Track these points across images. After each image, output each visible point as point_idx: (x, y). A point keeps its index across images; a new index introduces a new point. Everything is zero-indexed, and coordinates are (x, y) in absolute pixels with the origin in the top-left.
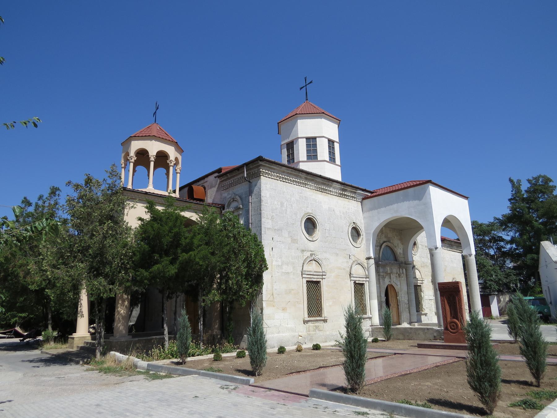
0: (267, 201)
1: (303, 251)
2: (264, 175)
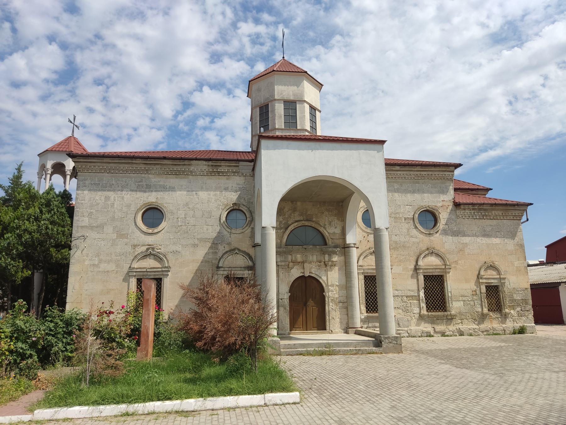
1: (135, 246)
2: (81, 171)
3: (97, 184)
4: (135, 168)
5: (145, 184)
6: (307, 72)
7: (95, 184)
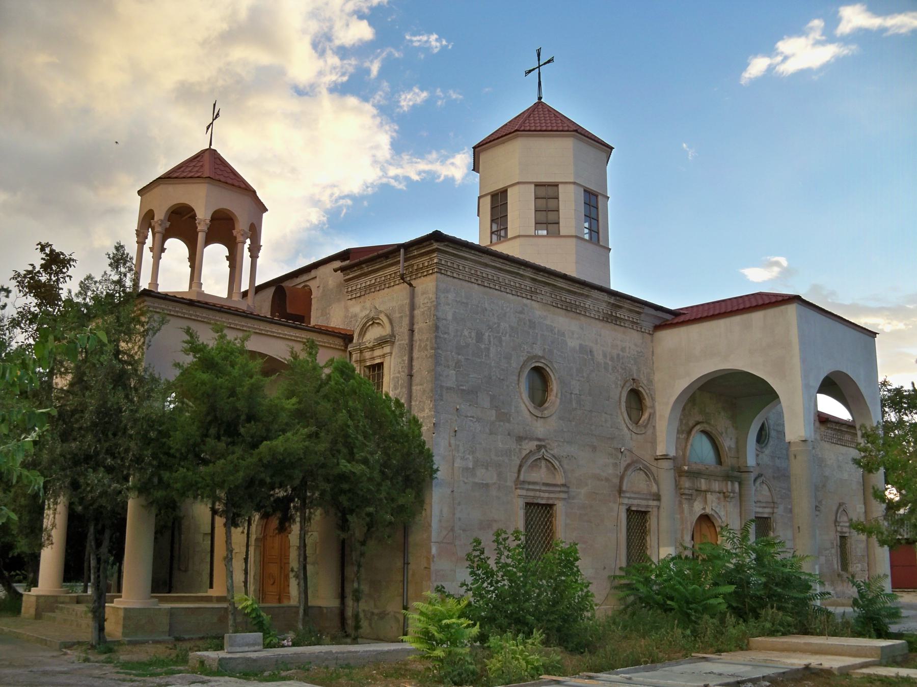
0: (448, 330)
1: (520, 439)
2: (443, 272)
3: (464, 303)
4: (517, 285)
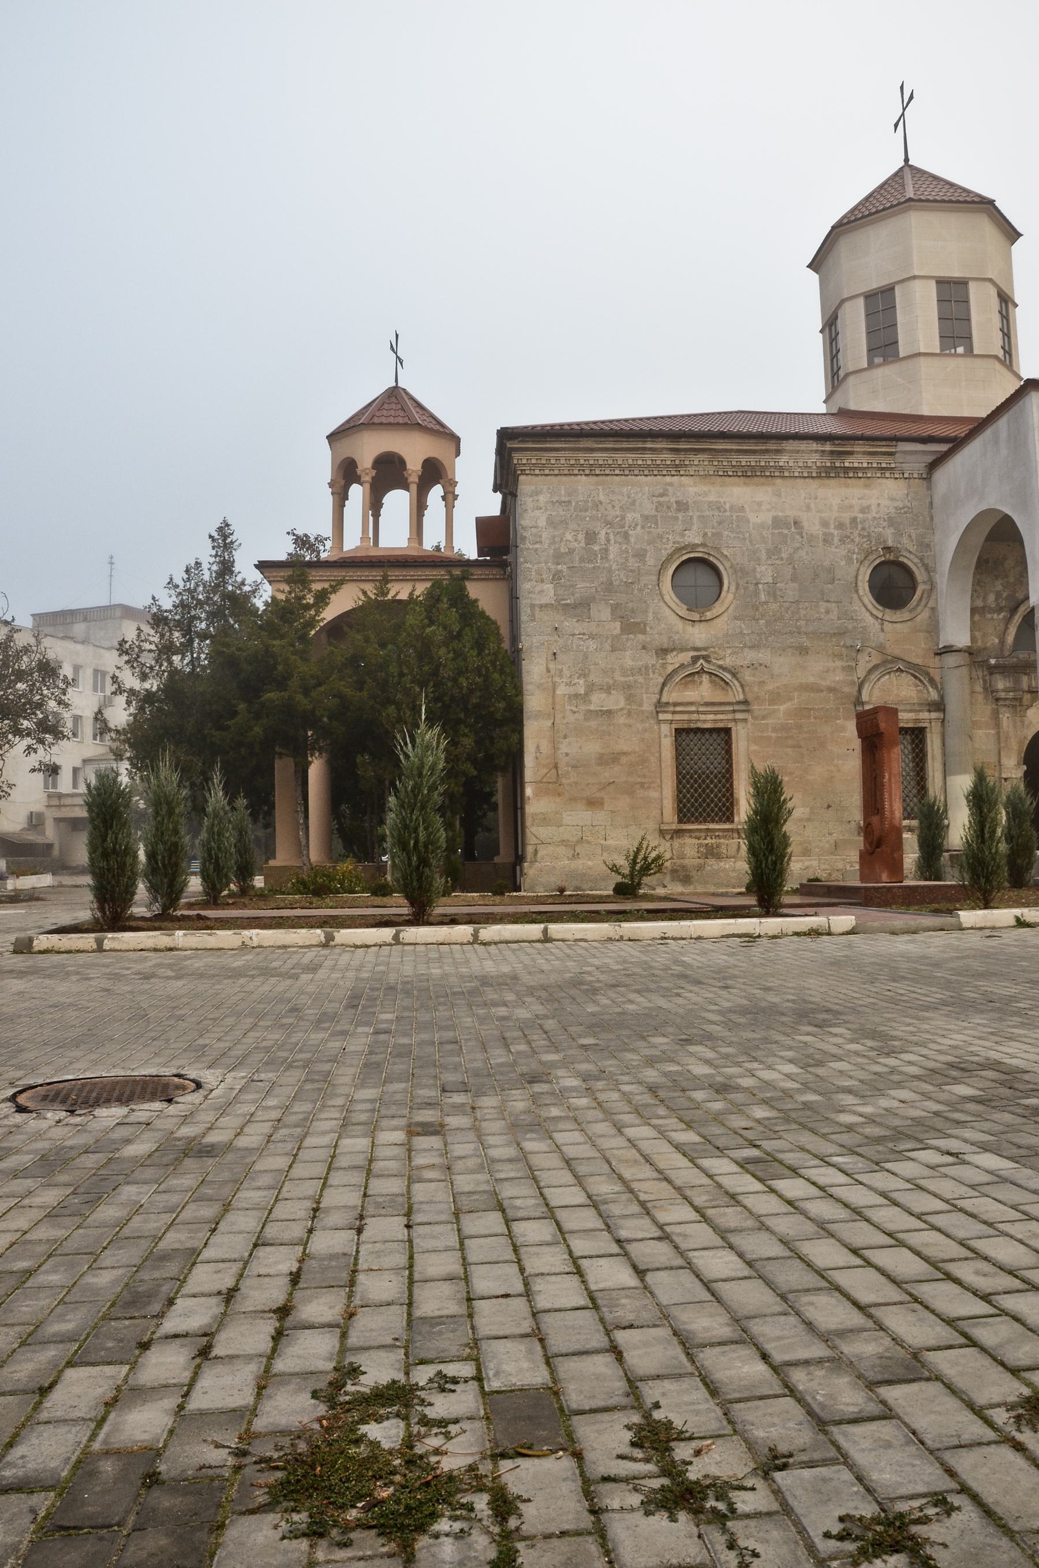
0: (540, 537)
1: (663, 652)
2: (527, 472)
4: (649, 462)
5: (673, 500)
6: (991, 202)
7: (560, 503)
